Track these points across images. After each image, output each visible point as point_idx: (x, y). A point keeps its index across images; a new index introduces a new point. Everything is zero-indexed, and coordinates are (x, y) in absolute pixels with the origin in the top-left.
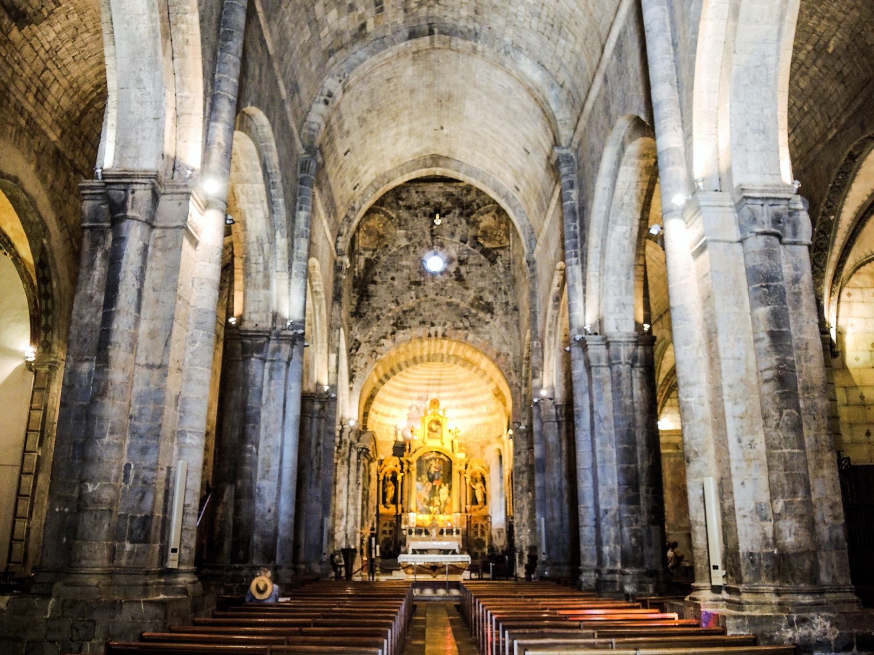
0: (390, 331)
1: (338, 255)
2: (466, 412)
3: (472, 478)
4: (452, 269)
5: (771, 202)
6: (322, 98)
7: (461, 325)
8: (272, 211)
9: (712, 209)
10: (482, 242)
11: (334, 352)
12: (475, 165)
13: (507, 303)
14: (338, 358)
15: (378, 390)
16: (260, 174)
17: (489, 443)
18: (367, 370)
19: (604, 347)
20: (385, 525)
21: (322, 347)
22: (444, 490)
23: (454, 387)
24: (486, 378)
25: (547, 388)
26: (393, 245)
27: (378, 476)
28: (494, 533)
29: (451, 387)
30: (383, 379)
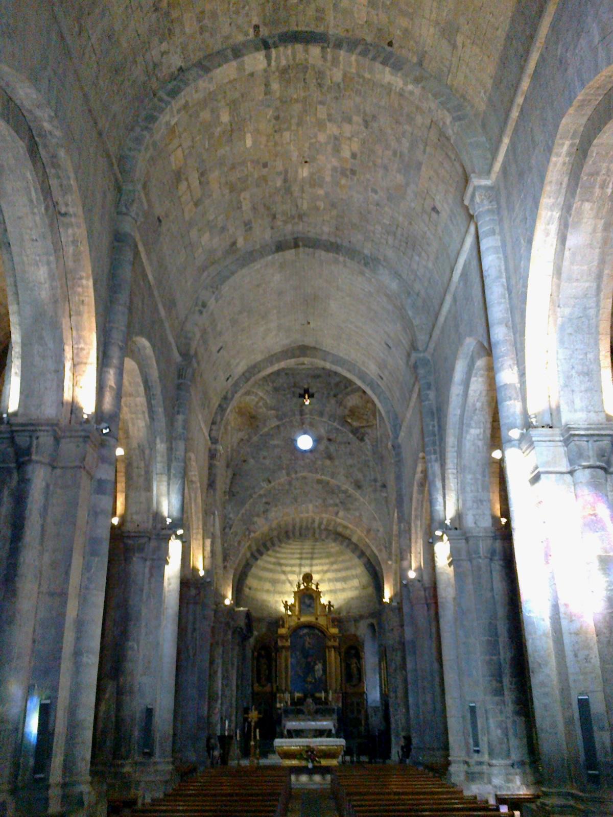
0: (262, 509)
1: (212, 443)
2: (339, 585)
4: (322, 447)
5: (596, 438)
6: (197, 308)
8: (152, 418)
9: (543, 444)
10: (349, 421)
11: (208, 538)
12: (341, 355)
13: (375, 480)
14: (213, 544)
15: (252, 566)
16: (141, 389)
19: (464, 541)
21: (197, 533)
22: (319, 667)
23: (327, 561)
25: (415, 571)
26: (264, 424)
28: (370, 711)
30: (256, 554)
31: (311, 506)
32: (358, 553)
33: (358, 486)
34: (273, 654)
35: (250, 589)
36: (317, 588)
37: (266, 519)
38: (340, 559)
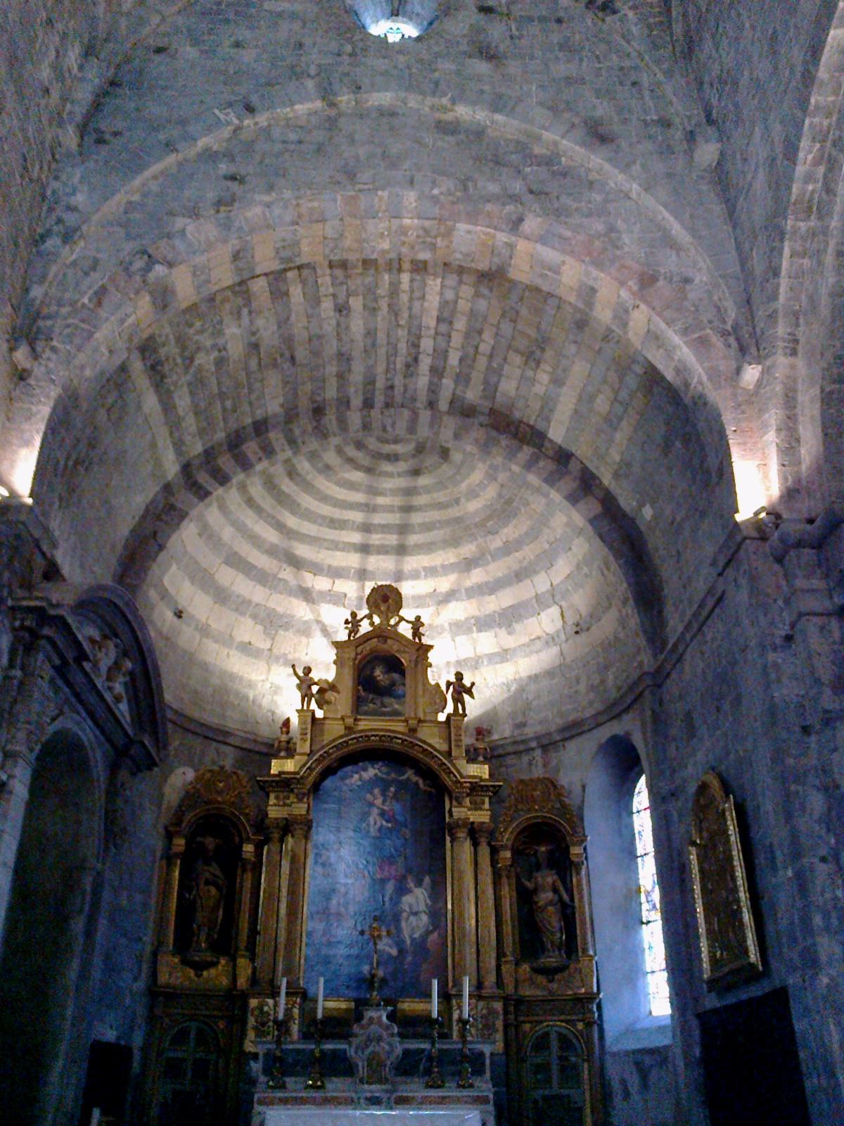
0: (211, 196)
7: (493, 188)
13: (666, 124)
15: (183, 516)
18: (103, 313)
28: (614, 1071)
31: (410, 197)
32: (569, 484)
33: (599, 135)
34: (248, 848)
35: (179, 614)
36: (416, 633)
37: (227, 226)
38: (496, 543)
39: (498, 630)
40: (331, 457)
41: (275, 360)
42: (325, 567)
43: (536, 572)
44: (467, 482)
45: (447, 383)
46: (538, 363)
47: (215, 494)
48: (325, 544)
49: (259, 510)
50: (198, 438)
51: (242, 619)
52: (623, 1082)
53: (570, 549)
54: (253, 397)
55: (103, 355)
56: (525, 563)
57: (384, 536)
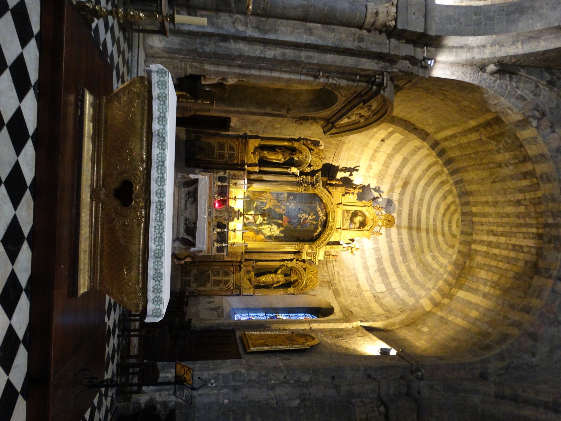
3: (291, 269)
15: (424, 140)
17: (336, 293)
20: (232, 149)
22: (276, 231)
23: (407, 248)
24: (438, 297)
27: (298, 140)
28: (216, 299)
29: (406, 242)
30: (439, 147)
35: (383, 140)
39: (376, 266)
40: (450, 199)
41: (494, 174)
42: (403, 198)
43: (400, 283)
44: (440, 256)
45: (484, 248)
46: (494, 287)
47: (433, 152)
48: (412, 197)
49: (427, 170)
50: (458, 144)
51: (381, 165)
52: (213, 302)
53: (410, 297)
54: (477, 166)
55: (493, 101)
56: (404, 278)
57: (416, 221)
